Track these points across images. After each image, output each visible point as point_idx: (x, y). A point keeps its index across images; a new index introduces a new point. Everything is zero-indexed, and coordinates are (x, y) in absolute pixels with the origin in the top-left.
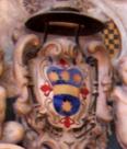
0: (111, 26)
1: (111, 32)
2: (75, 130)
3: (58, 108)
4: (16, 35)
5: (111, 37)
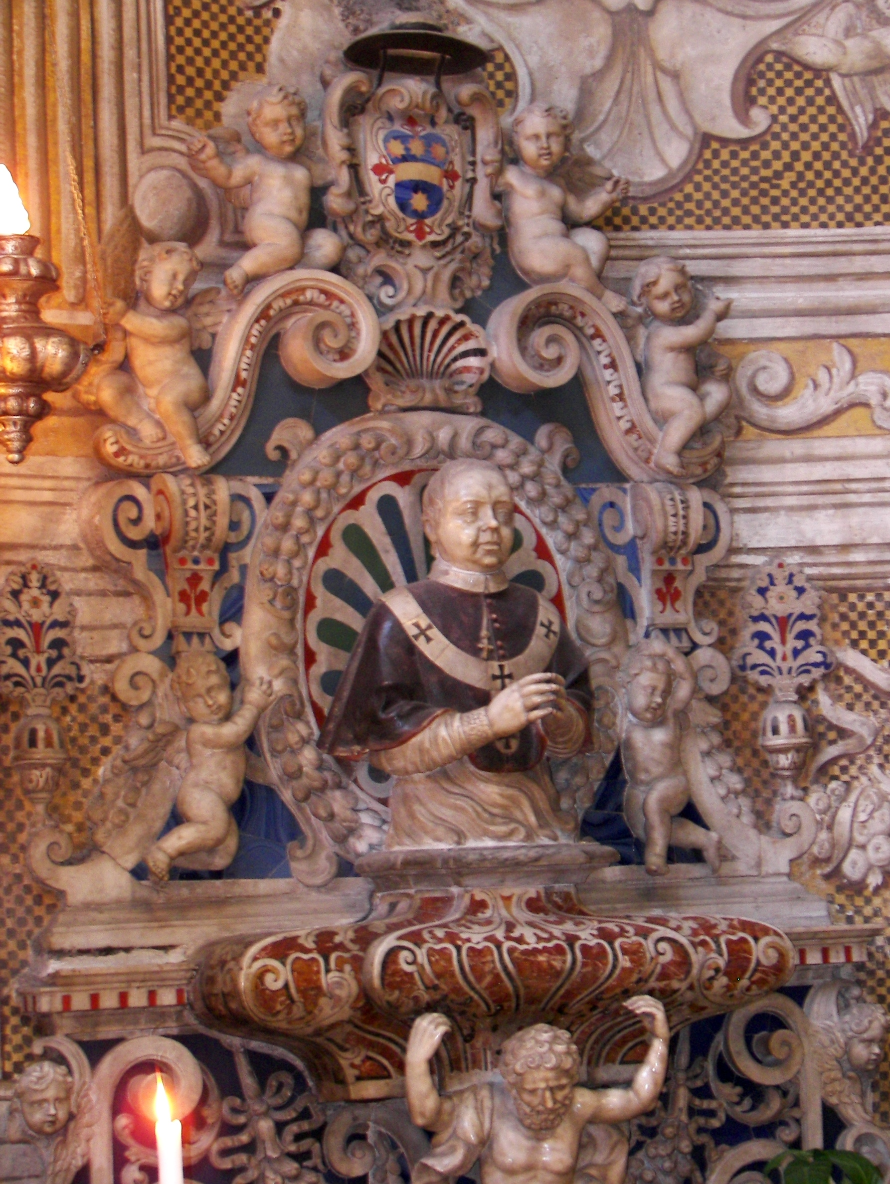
0: (499, 58)
1: (499, 67)
2: (435, 245)
3: (403, 205)
4: (328, 72)
5: (500, 76)
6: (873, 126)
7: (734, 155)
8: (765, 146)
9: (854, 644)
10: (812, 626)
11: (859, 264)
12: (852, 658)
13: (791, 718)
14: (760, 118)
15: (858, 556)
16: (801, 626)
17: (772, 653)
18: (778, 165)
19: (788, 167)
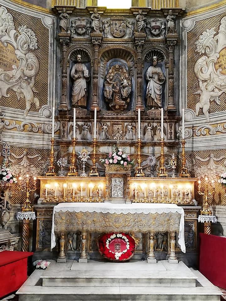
6: (20, 99)
7: (6, 99)
8: (9, 98)
9: (13, 153)
10: (9, 150)
11: (17, 113)
12: (13, 154)
13: (7, 160)
14: (9, 95)
15: (14, 143)
16: (8, 150)
17: (5, 153)
18: (10, 101)
19: (11, 101)
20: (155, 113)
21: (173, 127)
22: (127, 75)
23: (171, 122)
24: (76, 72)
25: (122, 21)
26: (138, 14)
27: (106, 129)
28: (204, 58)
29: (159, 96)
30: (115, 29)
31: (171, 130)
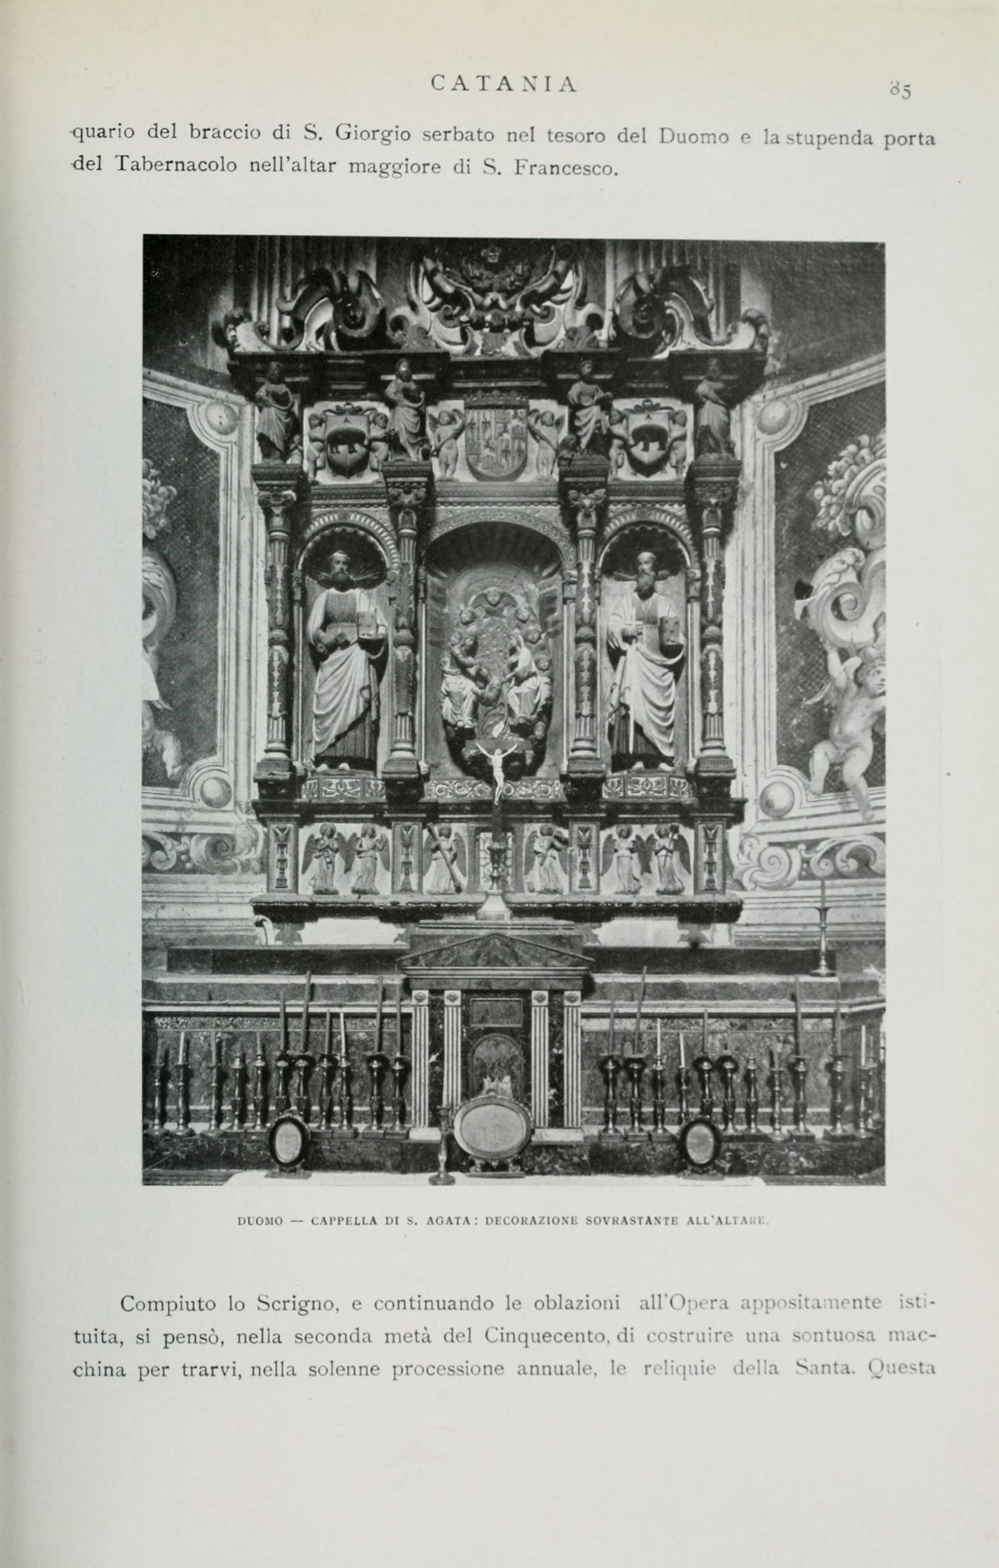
20: (648, 782)
21: (718, 841)
22: (533, 628)
23: (711, 819)
24: (328, 620)
25: (511, 412)
26: (574, 381)
27: (450, 850)
28: (848, 555)
29: (662, 714)
30: (483, 443)
31: (710, 854)
